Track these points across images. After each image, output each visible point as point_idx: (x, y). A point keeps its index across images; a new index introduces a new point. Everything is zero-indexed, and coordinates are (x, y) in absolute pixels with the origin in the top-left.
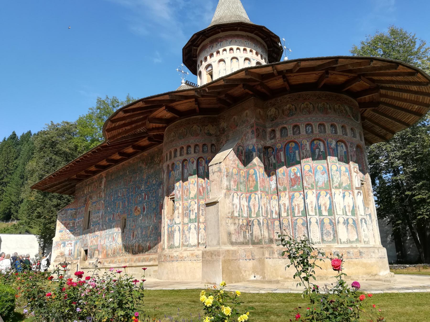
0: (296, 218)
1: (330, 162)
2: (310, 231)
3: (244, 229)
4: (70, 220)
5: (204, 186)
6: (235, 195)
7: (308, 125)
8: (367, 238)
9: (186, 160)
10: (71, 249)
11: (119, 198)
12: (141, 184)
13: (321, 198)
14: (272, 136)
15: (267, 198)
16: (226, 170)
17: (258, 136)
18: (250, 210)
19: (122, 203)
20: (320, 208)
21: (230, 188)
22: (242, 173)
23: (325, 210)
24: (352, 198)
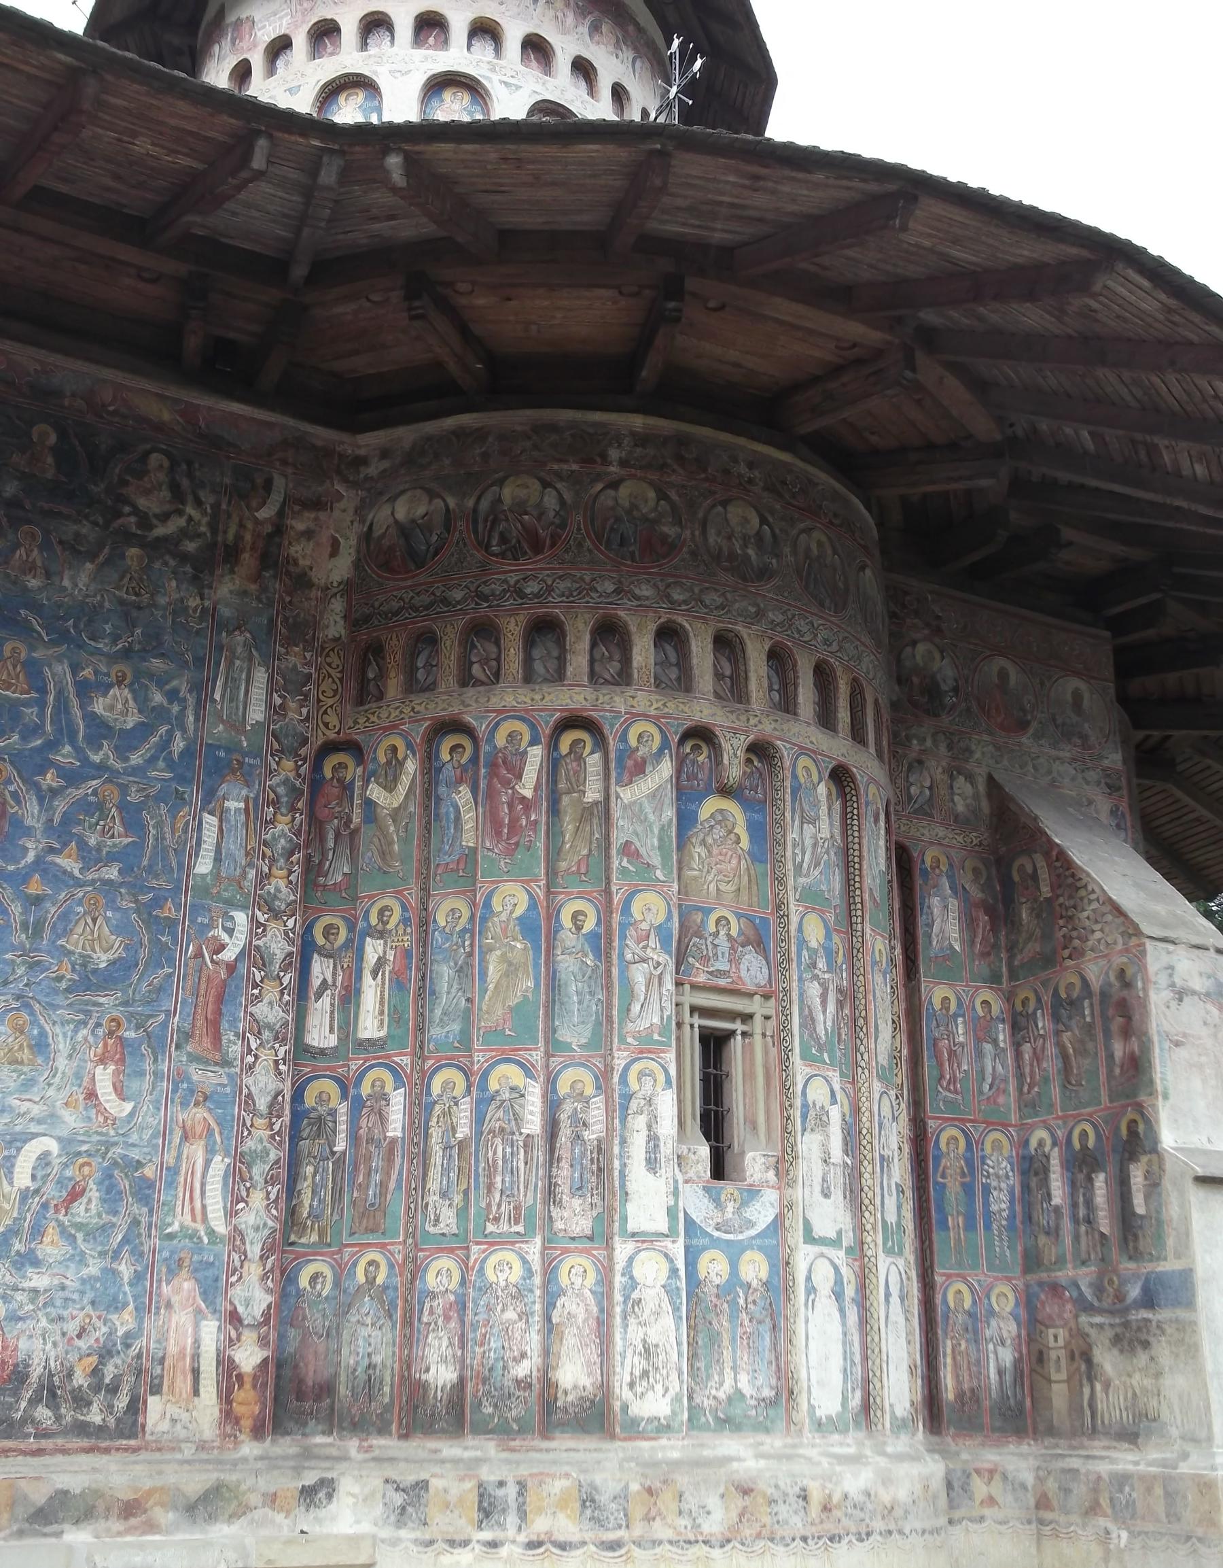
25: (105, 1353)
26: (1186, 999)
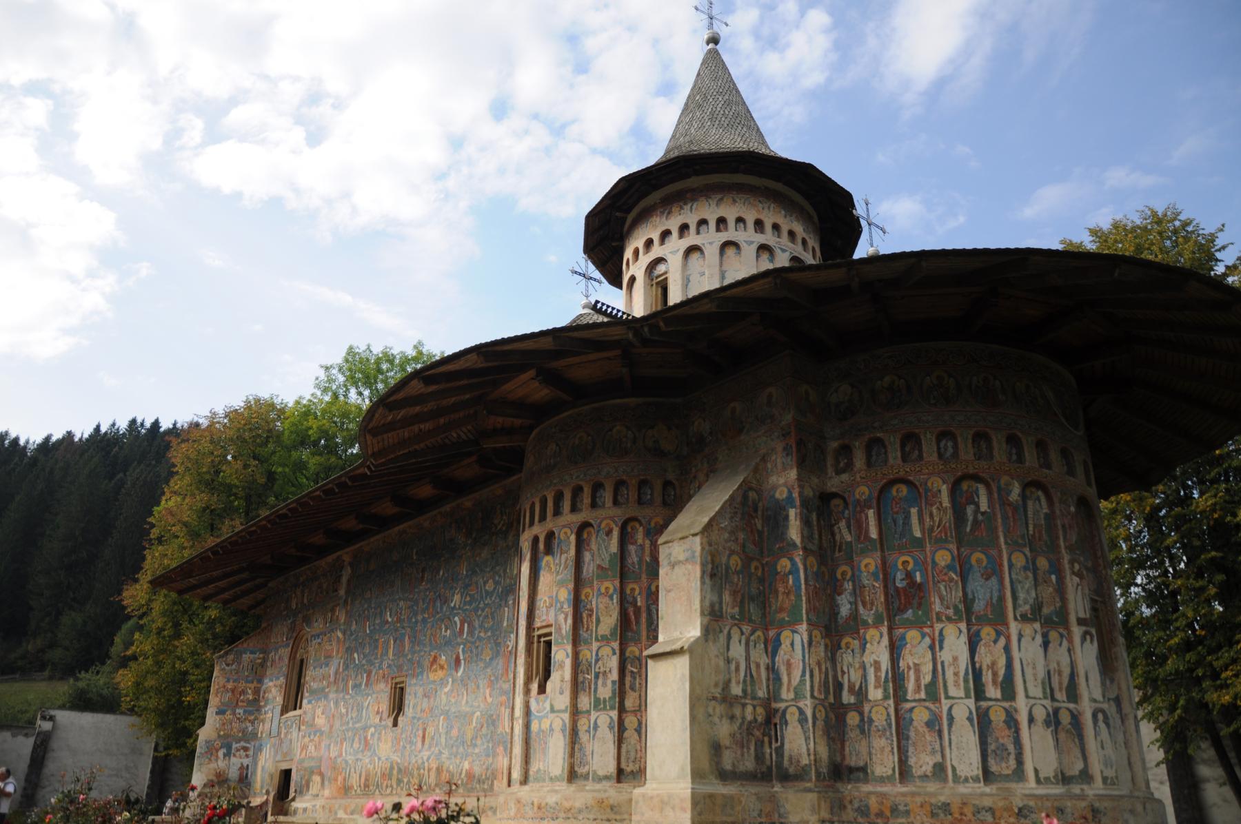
0: (908, 706)
1: (1006, 543)
2: (950, 743)
3: (757, 733)
4: (247, 682)
5: (639, 604)
6: (735, 631)
7: (942, 436)
8: (1112, 767)
9: (591, 525)
10: (245, 765)
11: (387, 626)
12: (451, 588)
13: (983, 648)
14: (842, 465)
15: (826, 646)
16: (709, 558)
17: (801, 464)
18: (778, 679)
19: (395, 642)
20: (977, 675)
21: (721, 612)
22: (756, 568)
23: (994, 682)
24: (1069, 650)
25: (487, 769)
26: (676, 567)
